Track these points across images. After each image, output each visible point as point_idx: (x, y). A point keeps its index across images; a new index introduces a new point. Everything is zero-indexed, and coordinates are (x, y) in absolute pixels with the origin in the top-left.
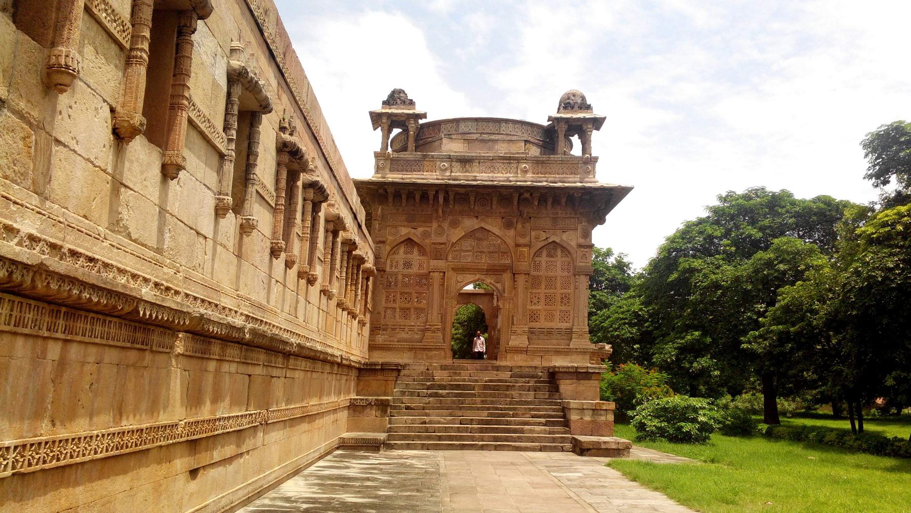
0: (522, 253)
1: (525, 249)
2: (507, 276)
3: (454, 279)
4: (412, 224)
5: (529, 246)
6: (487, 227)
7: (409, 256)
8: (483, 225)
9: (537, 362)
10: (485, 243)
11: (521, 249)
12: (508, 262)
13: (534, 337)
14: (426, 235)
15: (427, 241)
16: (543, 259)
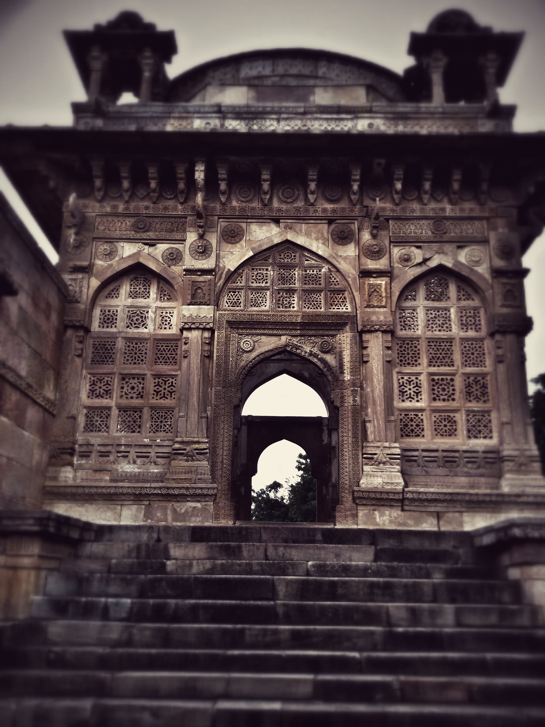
0: (374, 290)
1: (382, 282)
2: (345, 340)
3: (232, 348)
4: (144, 235)
5: (388, 273)
6: (301, 240)
7: (141, 302)
8: (290, 236)
9: (428, 525)
10: (297, 273)
11: (372, 281)
12: (347, 308)
13: (416, 470)
14: (174, 257)
15: (177, 269)
16: (421, 304)
